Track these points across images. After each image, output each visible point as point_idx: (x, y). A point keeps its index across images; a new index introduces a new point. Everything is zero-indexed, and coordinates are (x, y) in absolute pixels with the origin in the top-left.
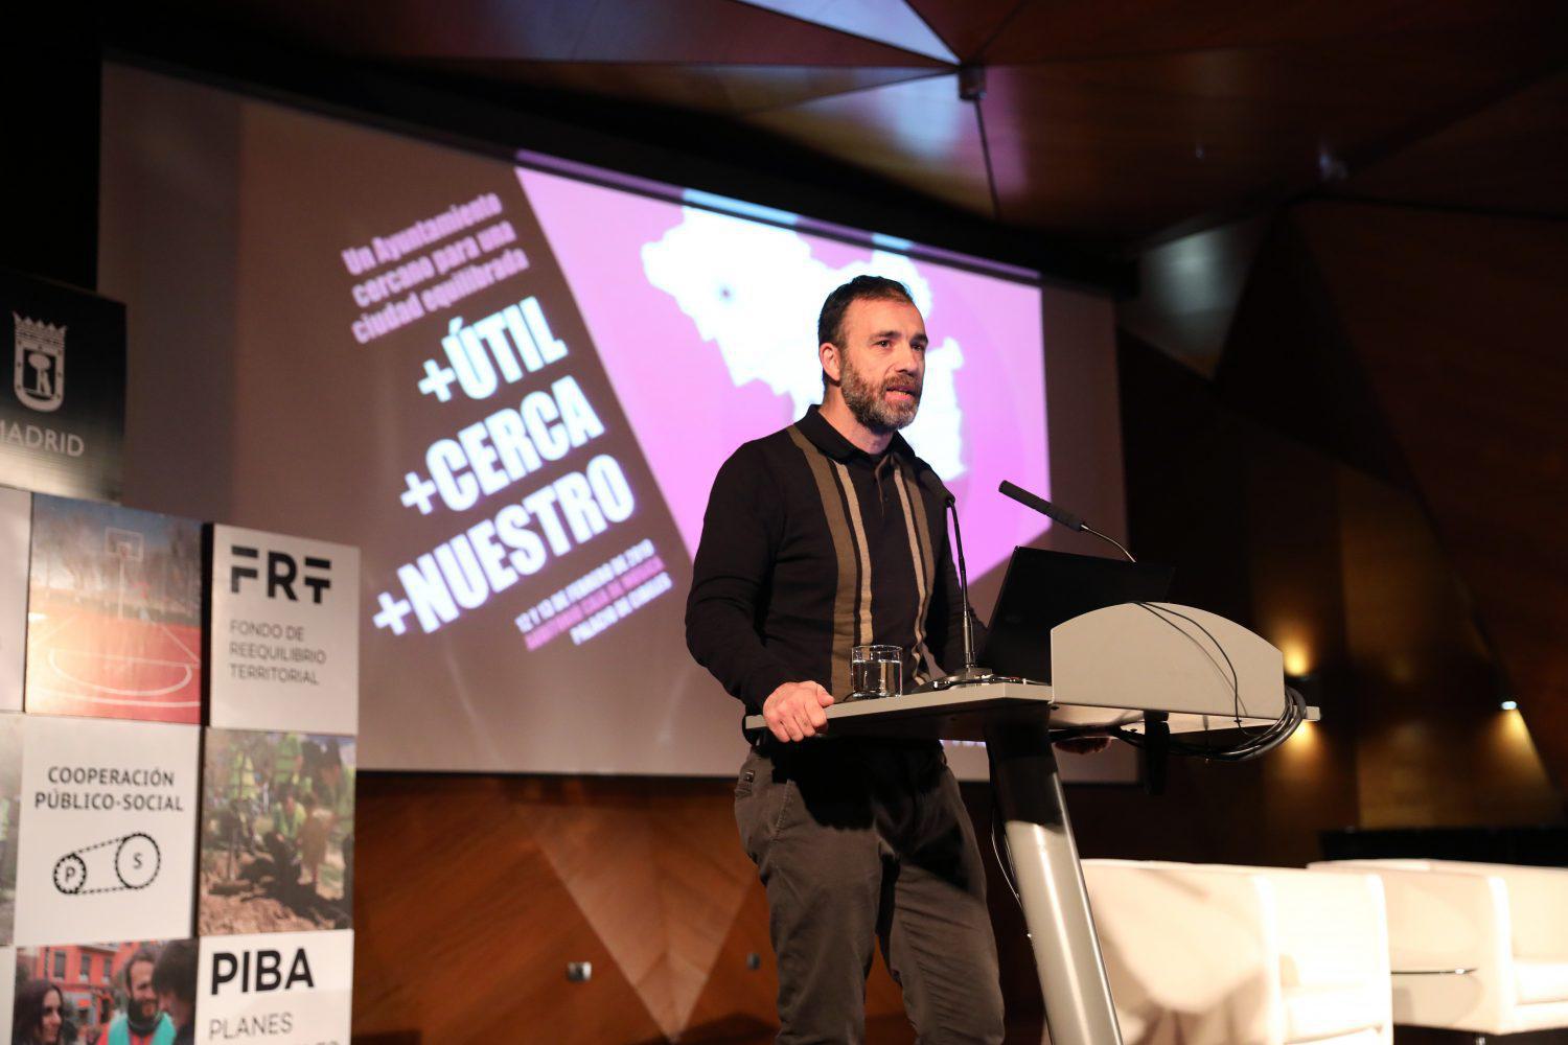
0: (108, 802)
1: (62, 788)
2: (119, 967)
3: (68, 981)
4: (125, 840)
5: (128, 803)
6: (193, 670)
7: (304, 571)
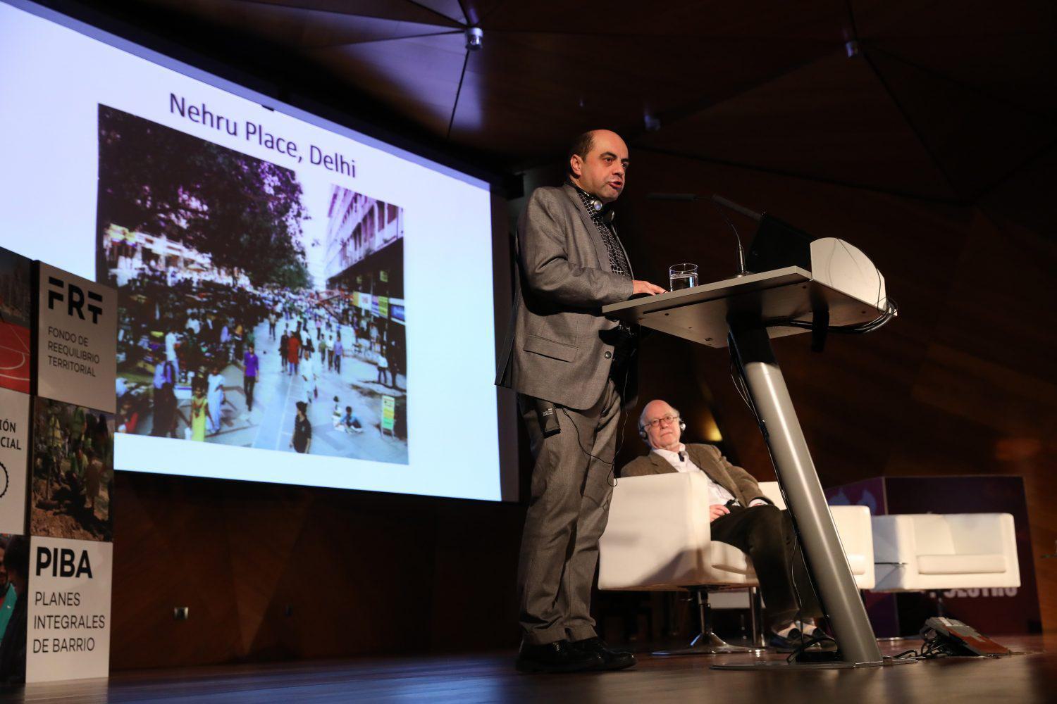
6: (26, 357)
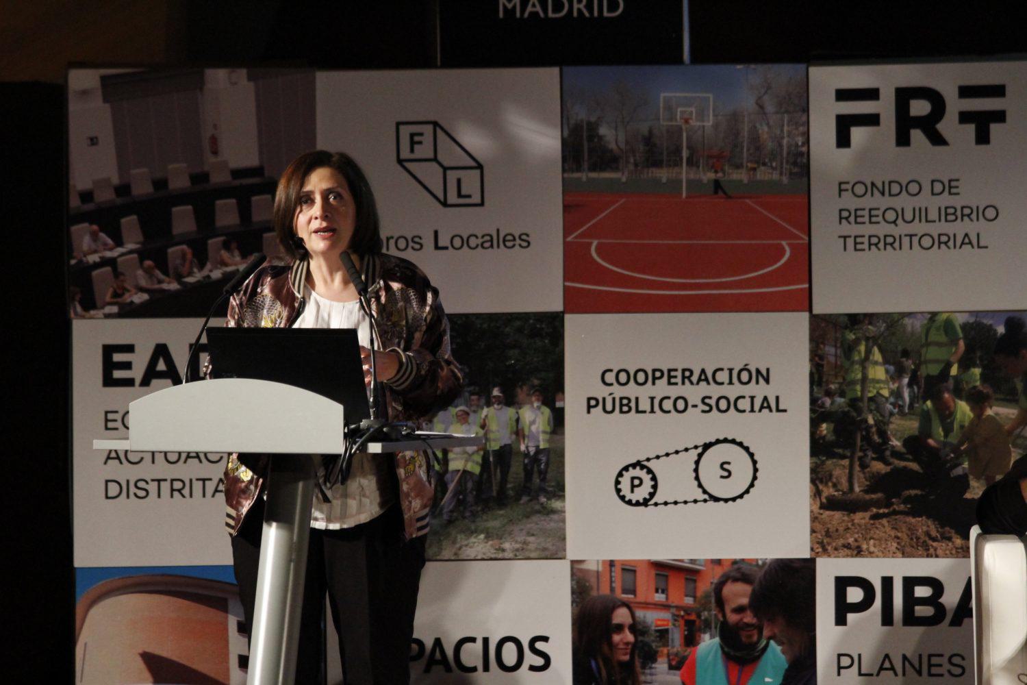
0: (681, 406)
1: (619, 391)
2: (705, 586)
3: (641, 597)
4: (707, 446)
5: (708, 405)
7: (955, 105)
